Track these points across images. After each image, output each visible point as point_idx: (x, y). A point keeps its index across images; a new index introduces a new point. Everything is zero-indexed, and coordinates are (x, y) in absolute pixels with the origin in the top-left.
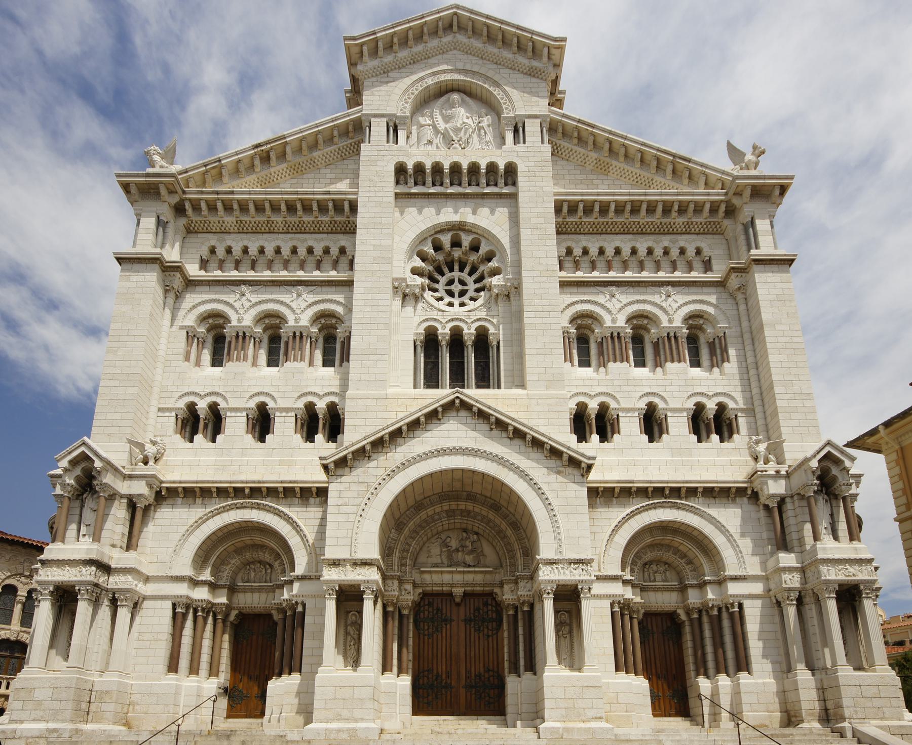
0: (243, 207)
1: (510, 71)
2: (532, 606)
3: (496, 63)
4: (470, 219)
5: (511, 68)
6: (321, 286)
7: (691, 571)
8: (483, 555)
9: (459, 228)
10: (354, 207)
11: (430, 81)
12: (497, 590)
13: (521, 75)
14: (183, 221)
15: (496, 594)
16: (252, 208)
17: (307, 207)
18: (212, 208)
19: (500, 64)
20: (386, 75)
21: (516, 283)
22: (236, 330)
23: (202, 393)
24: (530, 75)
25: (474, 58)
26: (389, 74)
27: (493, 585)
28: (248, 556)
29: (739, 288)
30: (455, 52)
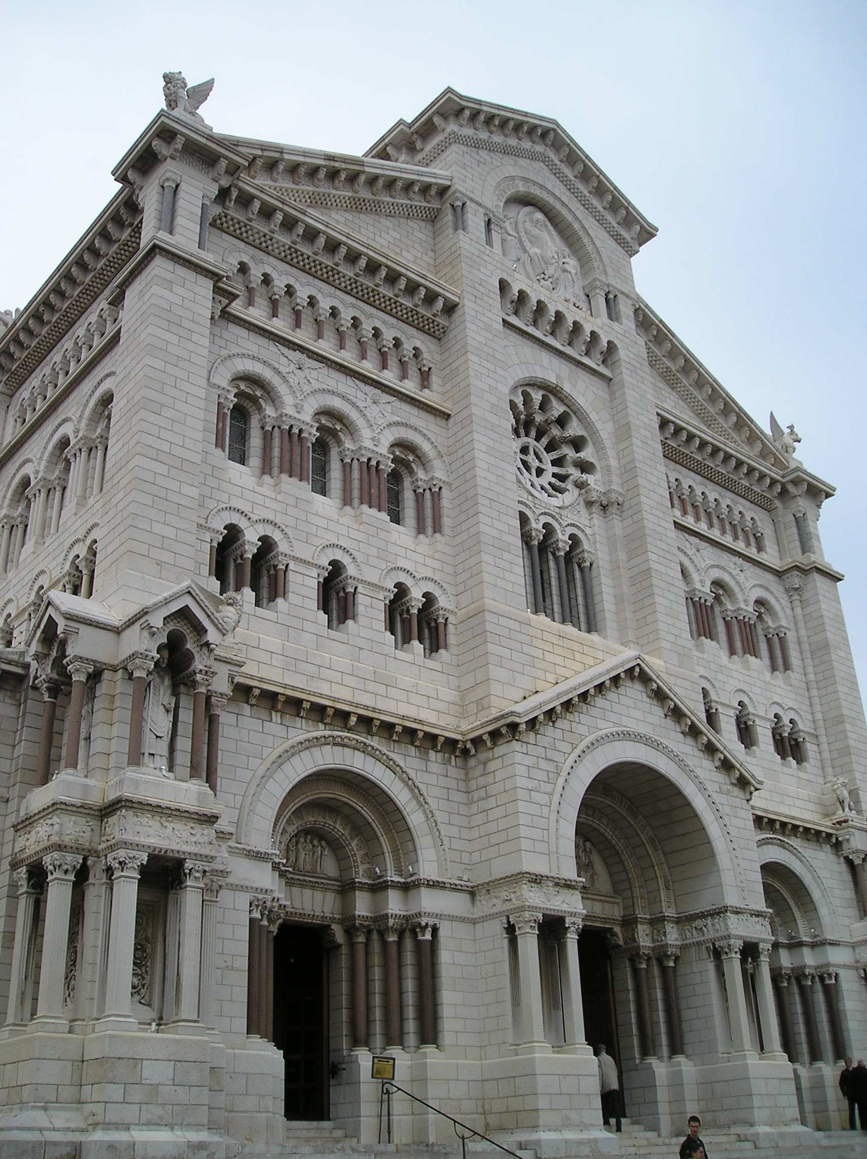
0: (311, 235)
1: (597, 223)
2: (677, 959)
3: (584, 205)
4: (567, 388)
5: (598, 221)
6: (401, 399)
7: (780, 926)
8: (596, 874)
9: (551, 391)
10: (450, 309)
11: (521, 188)
12: (617, 929)
13: (607, 235)
14: (217, 210)
15: (614, 934)
16: (321, 241)
17: (393, 278)
18: (267, 213)
19: (587, 209)
20: (476, 150)
21: (620, 500)
22: (293, 422)
23: (254, 518)
24: (616, 240)
25: (561, 184)
26: (479, 151)
27: (613, 921)
28: (310, 820)
29: (797, 589)
30: (542, 164)
